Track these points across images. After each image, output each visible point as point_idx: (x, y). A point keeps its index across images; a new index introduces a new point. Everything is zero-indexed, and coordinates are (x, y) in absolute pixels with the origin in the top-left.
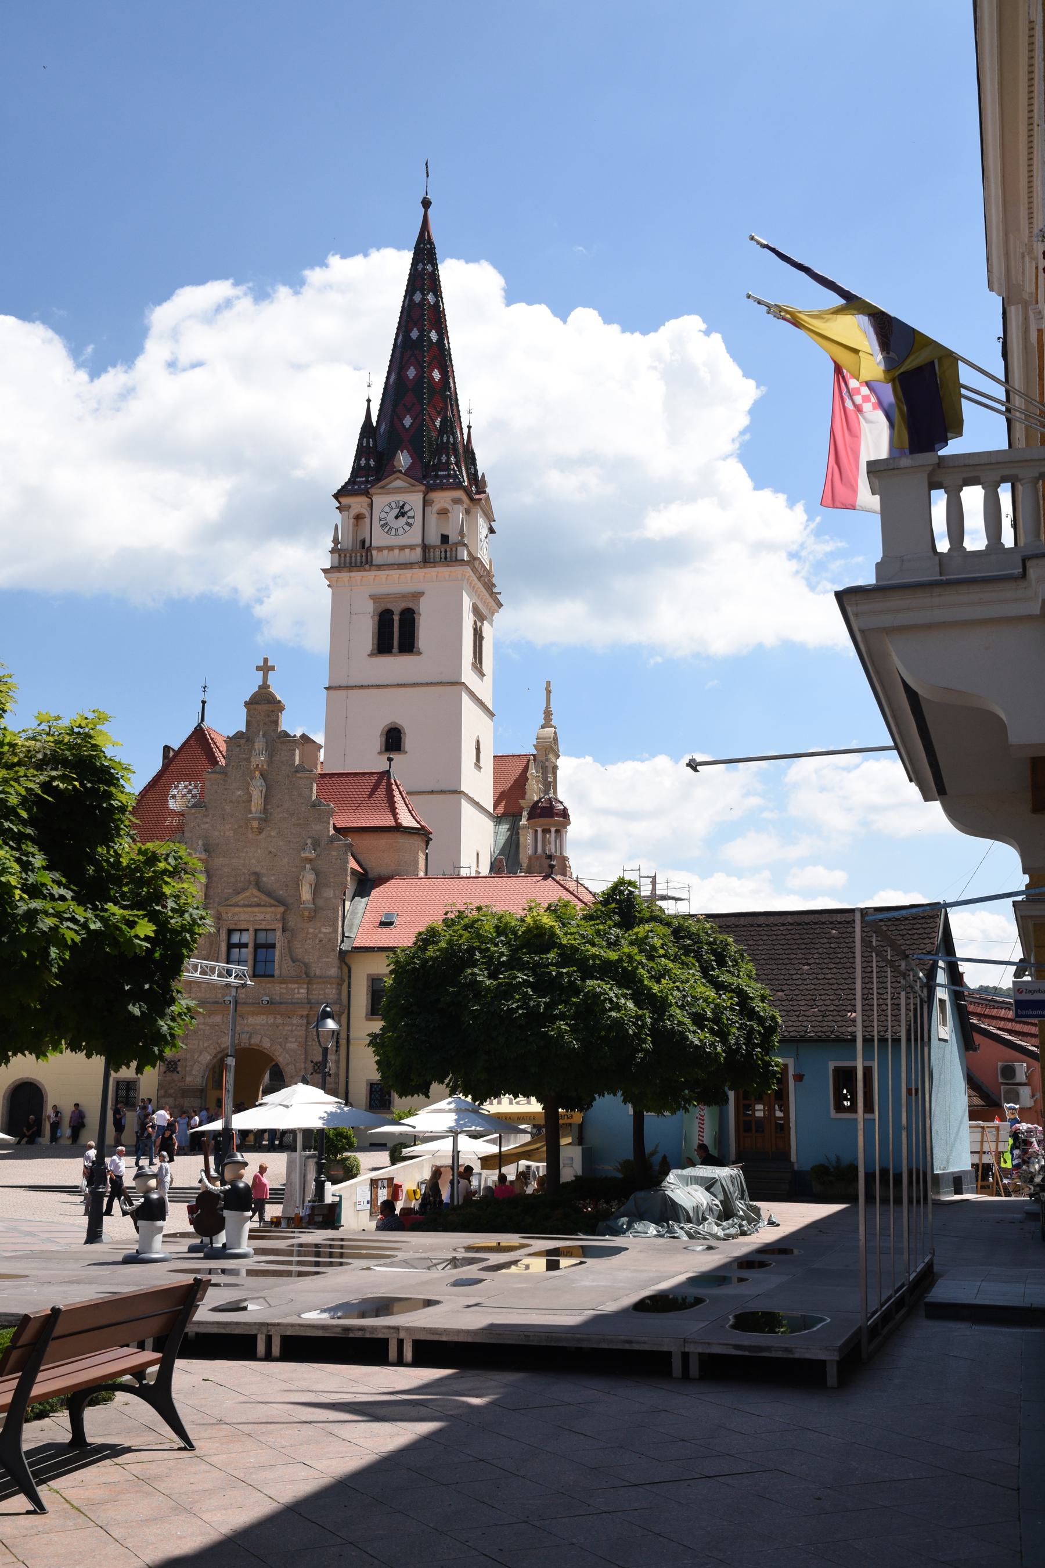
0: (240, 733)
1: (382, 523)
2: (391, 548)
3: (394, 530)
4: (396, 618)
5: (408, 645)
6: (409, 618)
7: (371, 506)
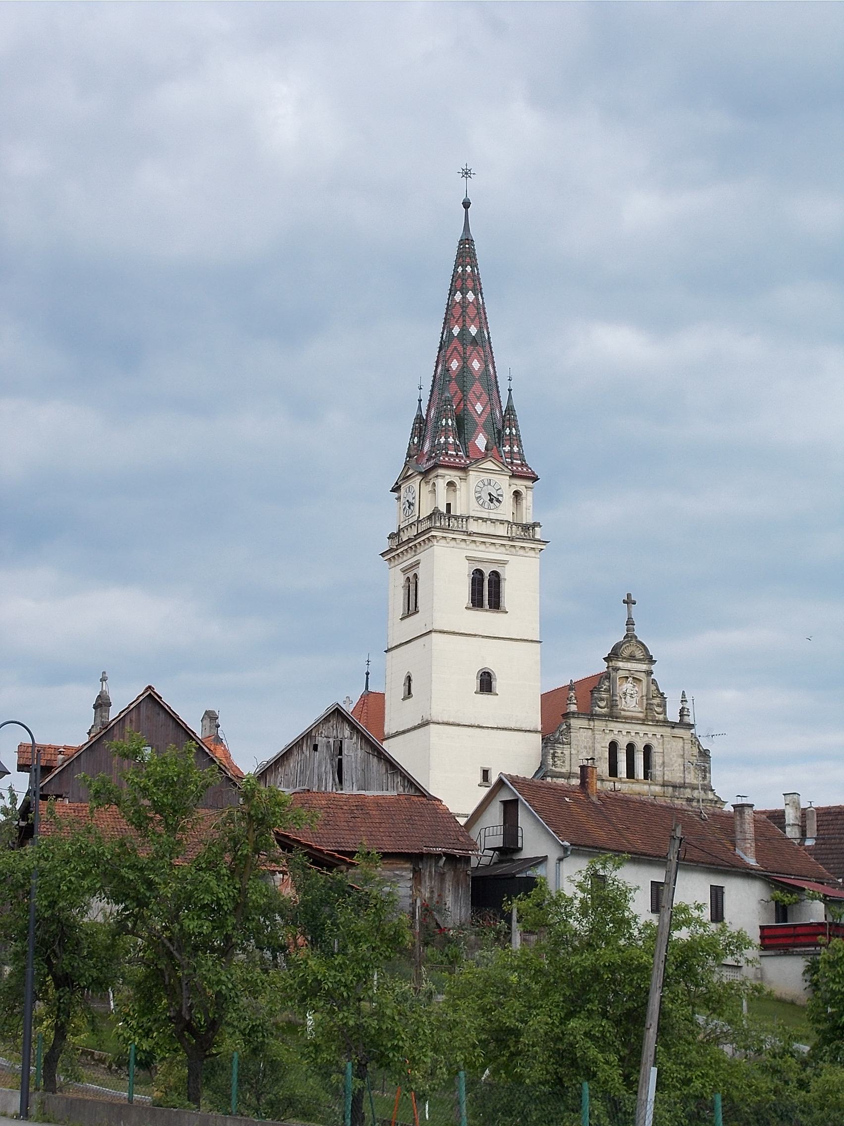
3: (482, 500)
5: (496, 604)
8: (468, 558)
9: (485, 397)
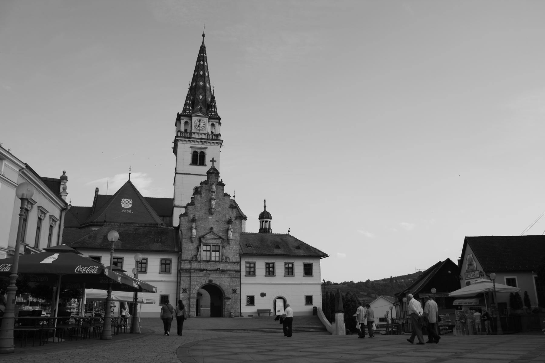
0: (206, 181)
1: (195, 125)
2: (198, 134)
4: (199, 155)
6: (203, 155)
7: (191, 120)
8: (191, 147)
9: (204, 94)
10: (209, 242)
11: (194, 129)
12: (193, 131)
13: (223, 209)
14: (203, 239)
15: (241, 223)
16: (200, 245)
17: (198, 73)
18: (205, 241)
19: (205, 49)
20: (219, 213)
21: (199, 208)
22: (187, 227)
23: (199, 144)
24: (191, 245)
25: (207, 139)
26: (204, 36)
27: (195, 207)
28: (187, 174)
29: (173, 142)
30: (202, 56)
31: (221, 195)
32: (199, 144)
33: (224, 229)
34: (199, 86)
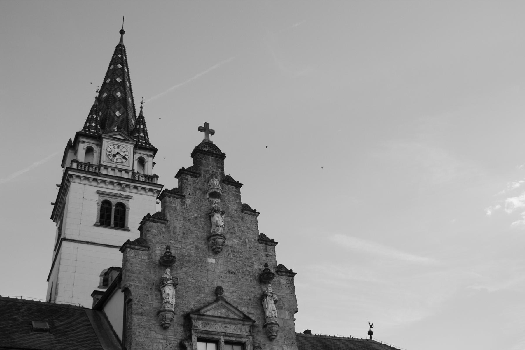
1: (108, 153)
2: (113, 169)
4: (113, 208)
8: (99, 193)
9: (123, 110)
10: (213, 329)
11: (107, 160)
12: (102, 163)
13: (244, 244)
14: (198, 319)
15: (292, 283)
16: (189, 338)
17: (112, 79)
18: (204, 325)
19: (125, 50)
20: (234, 252)
21: (178, 231)
22: (145, 279)
23: (115, 188)
24: (160, 336)
25: (133, 181)
26: (122, 32)
27: (169, 227)
28: (88, 243)
29: (57, 186)
30: (119, 58)
31: (233, 207)
32: (115, 188)
33: (252, 295)
34: (115, 98)
